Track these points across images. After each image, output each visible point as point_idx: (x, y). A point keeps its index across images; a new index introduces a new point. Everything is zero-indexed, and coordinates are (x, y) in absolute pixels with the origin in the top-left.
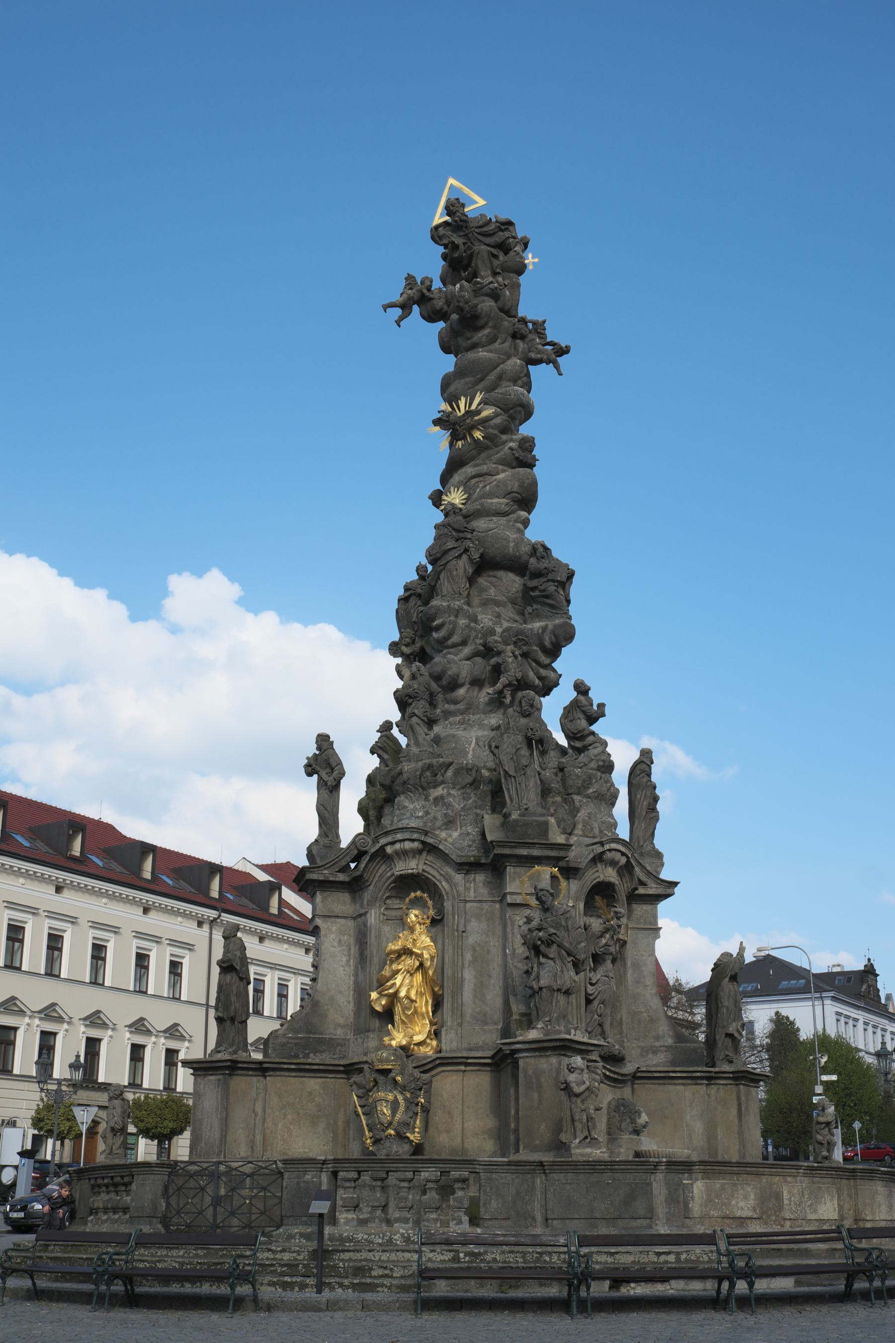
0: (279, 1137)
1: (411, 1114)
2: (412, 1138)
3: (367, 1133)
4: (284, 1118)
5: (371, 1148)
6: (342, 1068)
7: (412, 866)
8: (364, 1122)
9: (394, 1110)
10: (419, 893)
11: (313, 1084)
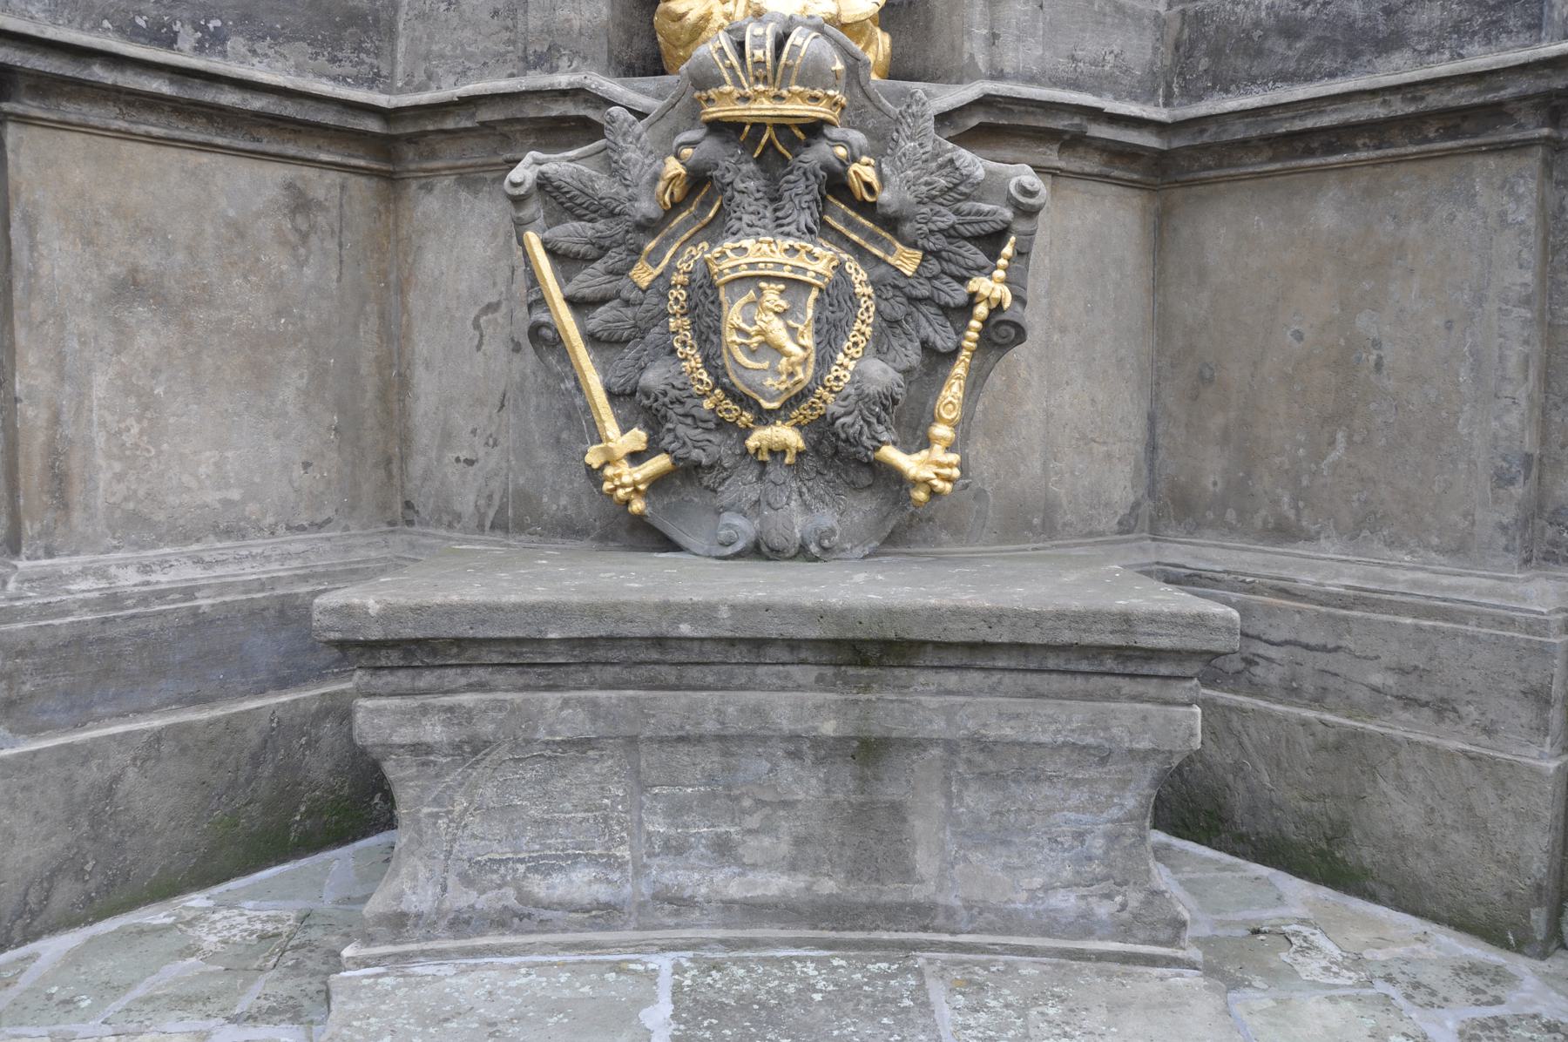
0: (100, 440)
2: (911, 464)
3: (611, 427)
4: (119, 348)
5: (638, 506)
6: (373, 125)
8: (594, 382)
9: (830, 333)
11: (247, 185)
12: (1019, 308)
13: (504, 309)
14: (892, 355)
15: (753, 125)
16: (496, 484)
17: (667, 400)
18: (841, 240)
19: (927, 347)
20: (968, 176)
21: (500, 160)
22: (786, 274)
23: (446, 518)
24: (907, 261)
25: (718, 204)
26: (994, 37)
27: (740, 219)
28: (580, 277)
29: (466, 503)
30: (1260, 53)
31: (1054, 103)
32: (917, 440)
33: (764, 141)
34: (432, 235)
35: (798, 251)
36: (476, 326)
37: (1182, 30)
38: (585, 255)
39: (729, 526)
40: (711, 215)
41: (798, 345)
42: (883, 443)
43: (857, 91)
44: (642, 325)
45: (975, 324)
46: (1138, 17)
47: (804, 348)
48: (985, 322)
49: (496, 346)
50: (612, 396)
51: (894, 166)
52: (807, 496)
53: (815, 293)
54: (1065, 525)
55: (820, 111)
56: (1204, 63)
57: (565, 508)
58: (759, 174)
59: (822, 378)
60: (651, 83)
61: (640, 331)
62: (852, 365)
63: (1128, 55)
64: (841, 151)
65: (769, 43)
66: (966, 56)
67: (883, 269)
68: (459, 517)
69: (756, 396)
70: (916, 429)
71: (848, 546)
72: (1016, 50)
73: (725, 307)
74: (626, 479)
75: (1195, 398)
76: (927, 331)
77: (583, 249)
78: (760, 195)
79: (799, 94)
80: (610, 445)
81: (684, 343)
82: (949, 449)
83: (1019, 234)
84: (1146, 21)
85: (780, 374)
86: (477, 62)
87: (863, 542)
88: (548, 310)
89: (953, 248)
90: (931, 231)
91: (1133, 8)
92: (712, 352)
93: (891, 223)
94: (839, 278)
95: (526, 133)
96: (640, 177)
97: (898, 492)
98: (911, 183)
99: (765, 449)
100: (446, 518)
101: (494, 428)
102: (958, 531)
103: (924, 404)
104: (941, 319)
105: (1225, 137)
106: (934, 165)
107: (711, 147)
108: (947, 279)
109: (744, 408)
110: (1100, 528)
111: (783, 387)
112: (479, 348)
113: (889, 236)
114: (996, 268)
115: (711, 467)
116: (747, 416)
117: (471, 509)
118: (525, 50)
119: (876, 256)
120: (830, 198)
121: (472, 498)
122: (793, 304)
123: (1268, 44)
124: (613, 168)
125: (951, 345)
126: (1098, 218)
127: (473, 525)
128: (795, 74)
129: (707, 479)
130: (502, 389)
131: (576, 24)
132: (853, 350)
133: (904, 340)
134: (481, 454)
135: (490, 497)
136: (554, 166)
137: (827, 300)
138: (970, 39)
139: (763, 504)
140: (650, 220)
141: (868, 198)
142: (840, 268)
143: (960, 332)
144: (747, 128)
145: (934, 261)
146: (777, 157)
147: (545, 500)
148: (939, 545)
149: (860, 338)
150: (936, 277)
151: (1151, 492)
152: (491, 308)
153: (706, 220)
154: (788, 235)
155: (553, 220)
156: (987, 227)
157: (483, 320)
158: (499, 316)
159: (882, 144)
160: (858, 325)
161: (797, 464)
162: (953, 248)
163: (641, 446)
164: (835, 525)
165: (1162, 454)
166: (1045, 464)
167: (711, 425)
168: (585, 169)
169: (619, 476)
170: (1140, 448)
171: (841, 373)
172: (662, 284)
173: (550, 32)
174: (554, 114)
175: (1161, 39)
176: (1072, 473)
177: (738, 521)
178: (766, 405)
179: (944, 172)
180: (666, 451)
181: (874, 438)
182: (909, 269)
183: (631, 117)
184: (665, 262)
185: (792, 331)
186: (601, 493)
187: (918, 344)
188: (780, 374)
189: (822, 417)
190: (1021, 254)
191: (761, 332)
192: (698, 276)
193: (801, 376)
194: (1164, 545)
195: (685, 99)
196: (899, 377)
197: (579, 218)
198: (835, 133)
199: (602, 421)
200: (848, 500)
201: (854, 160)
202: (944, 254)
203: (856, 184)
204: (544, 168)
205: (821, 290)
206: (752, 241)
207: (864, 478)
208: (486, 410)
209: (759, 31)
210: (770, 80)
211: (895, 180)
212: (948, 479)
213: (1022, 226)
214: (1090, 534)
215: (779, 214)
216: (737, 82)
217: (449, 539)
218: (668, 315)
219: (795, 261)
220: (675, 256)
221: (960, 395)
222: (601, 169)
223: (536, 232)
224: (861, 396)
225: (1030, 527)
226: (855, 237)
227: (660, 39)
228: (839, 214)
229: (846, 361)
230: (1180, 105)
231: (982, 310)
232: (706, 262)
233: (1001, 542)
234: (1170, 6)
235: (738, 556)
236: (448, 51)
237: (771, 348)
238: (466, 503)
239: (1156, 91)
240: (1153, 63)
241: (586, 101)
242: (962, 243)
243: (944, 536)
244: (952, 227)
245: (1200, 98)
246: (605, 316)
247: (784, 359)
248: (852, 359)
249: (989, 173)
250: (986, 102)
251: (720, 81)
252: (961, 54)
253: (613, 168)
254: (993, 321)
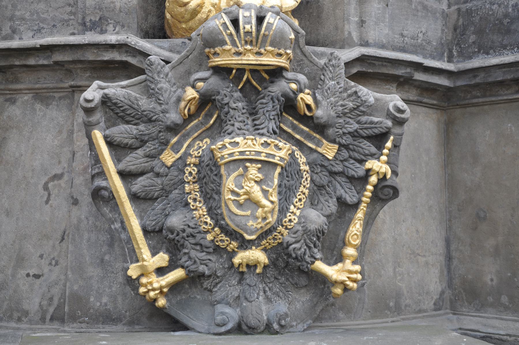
1: (332, 207)
2: (332, 272)
3: (145, 252)
5: (162, 302)
9: (286, 193)
12: (394, 178)
13: (66, 178)
14: (320, 206)
15: (238, 70)
16: (56, 291)
17: (185, 235)
18: (289, 138)
19: (341, 202)
20: (365, 101)
21: (66, 85)
22: (263, 158)
23: (16, 315)
24: (329, 151)
25: (215, 116)
26: (362, 22)
27: (233, 125)
28: (128, 159)
29: (33, 304)
30: (508, 32)
31: (398, 60)
33: (245, 79)
34: (14, 131)
35: (269, 144)
36: (46, 187)
37: (458, 20)
38: (131, 145)
39: (223, 313)
40: (212, 122)
41: (269, 202)
42: (316, 259)
43: (298, 51)
44: (168, 188)
45: (370, 187)
46: (434, 12)
47: (272, 202)
48: (375, 186)
49: (60, 201)
50: (146, 232)
51: (323, 95)
52: (269, 293)
53: (279, 170)
54: (406, 306)
55: (282, 62)
56: (473, 38)
57: (106, 304)
58: (243, 99)
59: (281, 220)
60: (165, 43)
61: (165, 192)
62: (298, 213)
63: (429, 34)
64: (294, 86)
65: (254, 21)
66: (346, 33)
67: (315, 155)
68: (26, 313)
69: (241, 232)
70: (333, 250)
71: (294, 324)
72: (375, 30)
73: (224, 178)
74: (156, 285)
75: (475, 229)
76: (341, 192)
77: (130, 142)
78: (244, 111)
79: (271, 52)
80: (145, 263)
81: (195, 200)
82: (354, 263)
83: (395, 135)
84: (438, 15)
85: (257, 218)
86: (48, 24)
87: (303, 321)
88: (106, 179)
89: (356, 143)
90: (344, 133)
91: (431, 7)
92: (214, 205)
93: (321, 128)
94: (292, 161)
95: (85, 70)
96: (169, 99)
97: (323, 289)
98: (333, 105)
99: (244, 264)
100: (16, 315)
101: (56, 254)
102: (349, 311)
103: (338, 235)
104: (349, 185)
105: (490, 80)
106: (345, 95)
107: (215, 82)
108: (352, 161)
109: (232, 239)
110: (425, 307)
111: (259, 226)
112: (47, 202)
113: (318, 136)
114: (382, 154)
115: (209, 276)
116: (234, 244)
117: (37, 307)
118: (84, 18)
119: (310, 148)
120: (284, 114)
121: (37, 300)
122: (266, 176)
123: (513, 27)
124: (150, 92)
125: (355, 200)
126: (416, 125)
127: (37, 318)
128: (269, 41)
129: (206, 284)
130: (62, 229)
131: (118, 5)
132: (299, 204)
133: (327, 197)
134: (46, 270)
135: (51, 299)
136: (113, 91)
137: (285, 174)
138: (349, 23)
139: (242, 299)
140: (177, 125)
141: (308, 113)
142: (292, 155)
143: (360, 192)
144: (234, 71)
145: (345, 151)
146: (253, 90)
147: (92, 299)
148: (339, 320)
149: (302, 196)
150: (345, 160)
151: (450, 285)
152: (57, 177)
153: (208, 126)
154: (262, 135)
155: (110, 123)
156: (376, 131)
157: (50, 185)
158: (62, 182)
159: (315, 83)
160: (302, 189)
161: (263, 273)
162: (356, 143)
163: (165, 264)
164: (287, 310)
165: (455, 262)
166: (394, 269)
167: (211, 250)
168: (133, 93)
169: (151, 283)
170: (442, 259)
171: (293, 217)
172: (181, 164)
173: (101, 9)
174: (106, 59)
175: (445, 25)
176: (408, 274)
177: (228, 310)
178: (248, 237)
179: (351, 99)
180: (183, 267)
181: (312, 256)
182: (330, 156)
183: (163, 63)
184: (183, 150)
185: (265, 193)
186: (138, 294)
187: (335, 199)
188: (257, 218)
189: (280, 244)
190: (396, 146)
191: (247, 193)
192: (206, 159)
193: (271, 219)
194: (462, 317)
195: (195, 53)
196: (325, 219)
197: (128, 122)
198: (289, 75)
199: (140, 249)
200: (294, 295)
201: (301, 91)
202: (351, 146)
203: (302, 105)
204: (106, 91)
205: (282, 168)
206: (242, 138)
207: (303, 281)
208: (51, 243)
209: (247, 14)
210: (254, 43)
211: (324, 103)
212: (355, 281)
213: (397, 130)
214: (420, 311)
215: (257, 122)
216: (234, 44)
217: (18, 329)
218: (184, 182)
219: (267, 150)
220: (189, 147)
221: (361, 229)
222: (142, 93)
223: (100, 131)
224: (306, 231)
225: (389, 308)
226: (298, 137)
227: (168, 16)
228: (289, 123)
229: (295, 210)
230: (458, 62)
231: (374, 179)
232: (212, 151)
233: (373, 317)
234: (449, 6)
235: (228, 332)
236: (27, 15)
238: (33, 304)
239: (443, 54)
240: (441, 39)
241: (127, 52)
242: (361, 140)
243: (341, 315)
244: (356, 131)
245: (470, 58)
246: (143, 183)
247: (260, 210)
248: (298, 209)
249: (376, 100)
250: (362, 59)
251: (223, 43)
252: (343, 32)
253: (150, 92)
254: (380, 186)
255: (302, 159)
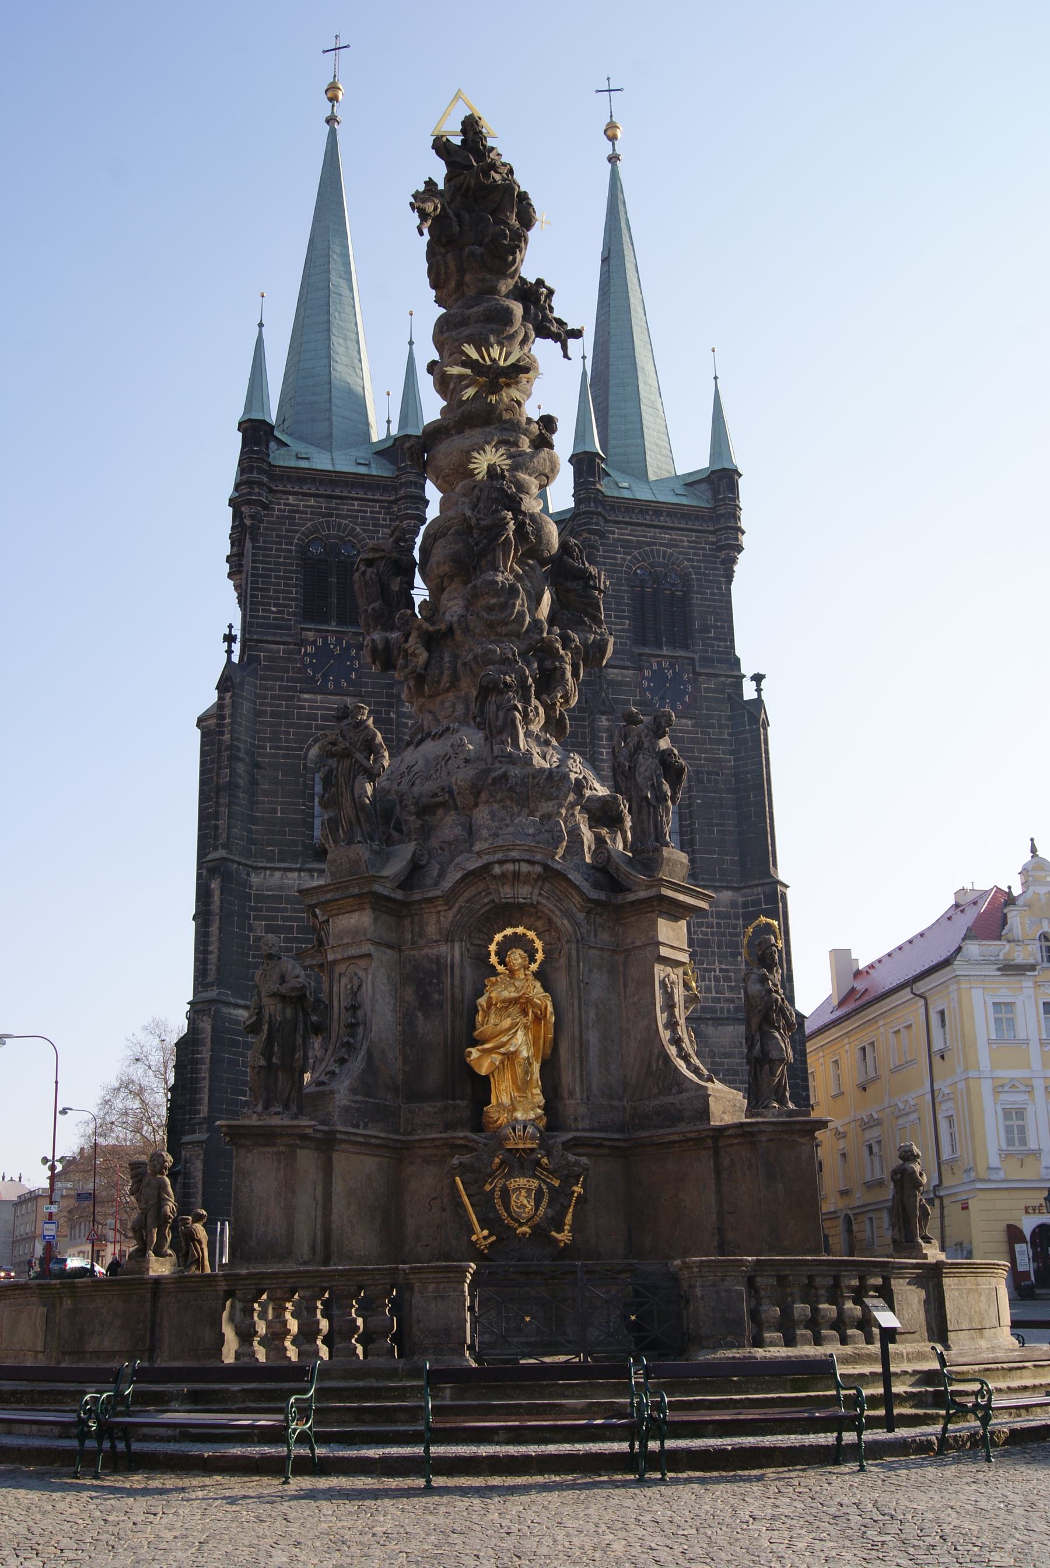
7: (524, 893)
10: (520, 930)
18: (539, 1178)
32: (560, 1230)
36: (429, 1203)
41: (530, 1206)
55: (534, 1146)
60: (483, 1135)
152: (435, 1198)
172: (493, 1190)
237: (523, 1206)
250: (575, 1138)
255: (544, 1187)
